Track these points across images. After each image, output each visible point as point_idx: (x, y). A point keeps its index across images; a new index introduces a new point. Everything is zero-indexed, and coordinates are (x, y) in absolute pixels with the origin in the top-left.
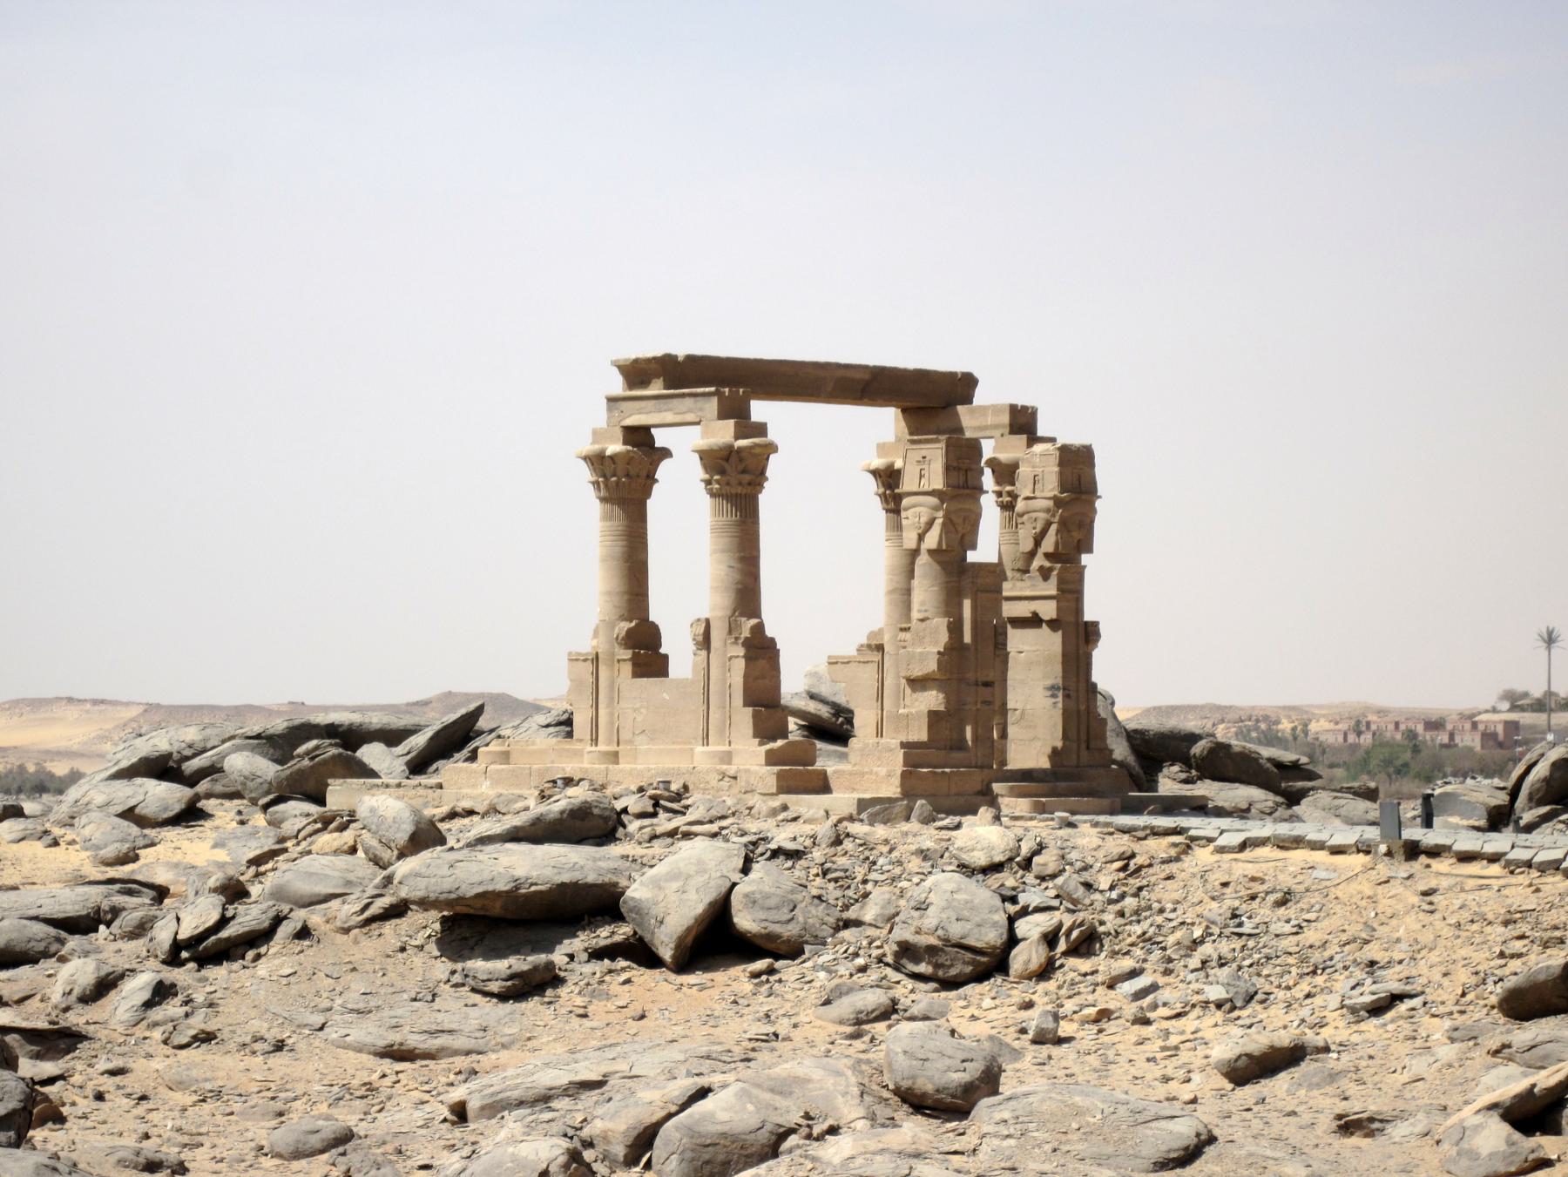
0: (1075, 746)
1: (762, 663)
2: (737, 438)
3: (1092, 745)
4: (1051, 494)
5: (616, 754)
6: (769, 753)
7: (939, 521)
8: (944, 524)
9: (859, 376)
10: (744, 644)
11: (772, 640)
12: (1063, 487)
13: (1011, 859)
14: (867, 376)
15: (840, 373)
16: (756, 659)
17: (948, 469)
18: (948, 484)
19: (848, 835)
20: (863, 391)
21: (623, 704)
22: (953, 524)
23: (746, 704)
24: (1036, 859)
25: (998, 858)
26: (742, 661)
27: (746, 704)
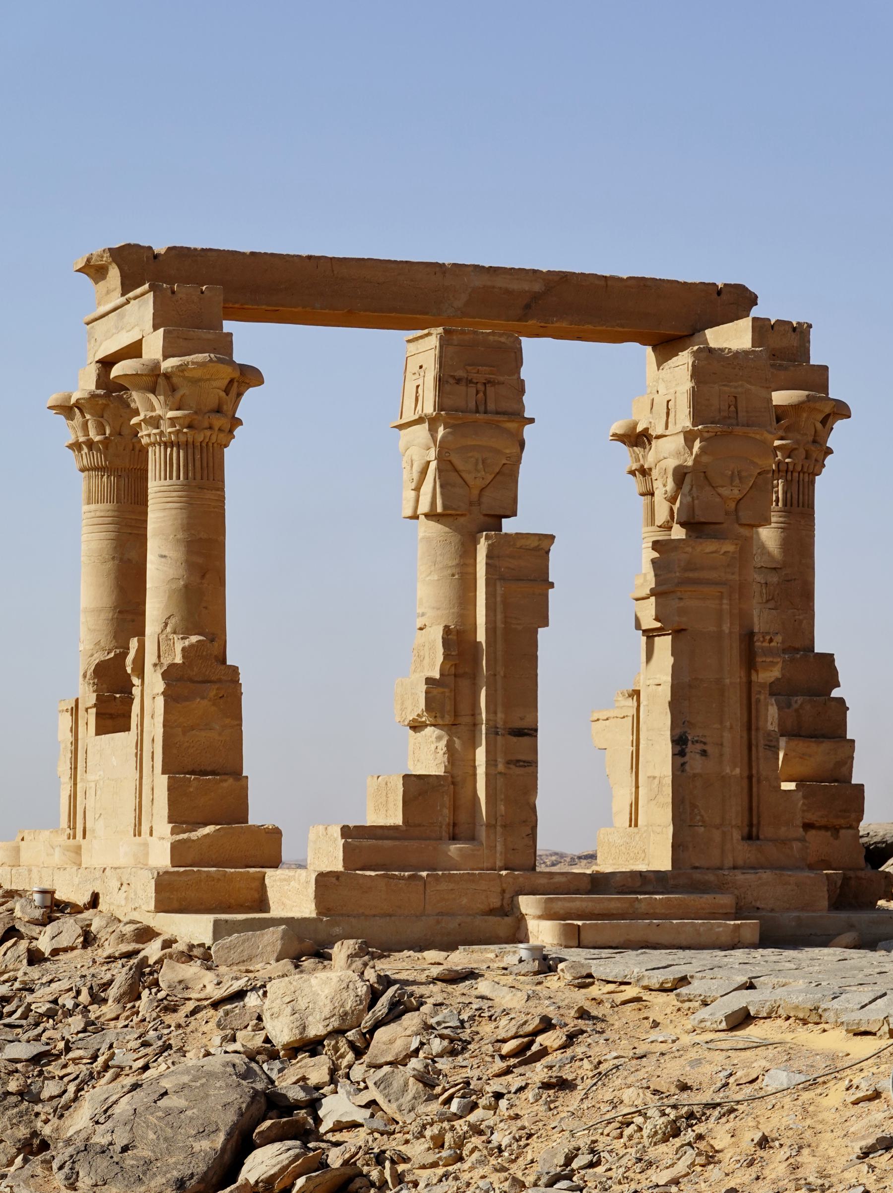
0: (717, 835)
1: (200, 706)
2: (165, 357)
3: (767, 831)
4: (679, 428)
5: (78, 850)
6: (175, 848)
7: (433, 465)
8: (440, 470)
9: (515, 286)
10: (164, 675)
11: (235, 670)
12: (697, 415)
13: (339, 1032)
14: (537, 287)
15: (479, 282)
16: (187, 699)
17: (441, 382)
18: (440, 406)
19: (156, 983)
20: (528, 307)
21: (90, 777)
22: (456, 470)
23: (163, 773)
24: (381, 1034)
25: (315, 1030)
26: (160, 701)
27: (163, 773)
